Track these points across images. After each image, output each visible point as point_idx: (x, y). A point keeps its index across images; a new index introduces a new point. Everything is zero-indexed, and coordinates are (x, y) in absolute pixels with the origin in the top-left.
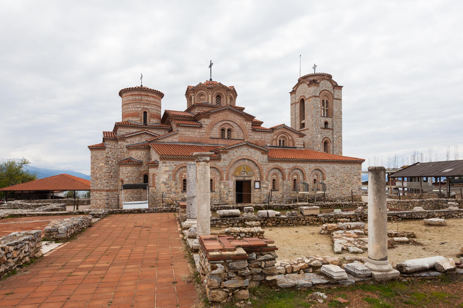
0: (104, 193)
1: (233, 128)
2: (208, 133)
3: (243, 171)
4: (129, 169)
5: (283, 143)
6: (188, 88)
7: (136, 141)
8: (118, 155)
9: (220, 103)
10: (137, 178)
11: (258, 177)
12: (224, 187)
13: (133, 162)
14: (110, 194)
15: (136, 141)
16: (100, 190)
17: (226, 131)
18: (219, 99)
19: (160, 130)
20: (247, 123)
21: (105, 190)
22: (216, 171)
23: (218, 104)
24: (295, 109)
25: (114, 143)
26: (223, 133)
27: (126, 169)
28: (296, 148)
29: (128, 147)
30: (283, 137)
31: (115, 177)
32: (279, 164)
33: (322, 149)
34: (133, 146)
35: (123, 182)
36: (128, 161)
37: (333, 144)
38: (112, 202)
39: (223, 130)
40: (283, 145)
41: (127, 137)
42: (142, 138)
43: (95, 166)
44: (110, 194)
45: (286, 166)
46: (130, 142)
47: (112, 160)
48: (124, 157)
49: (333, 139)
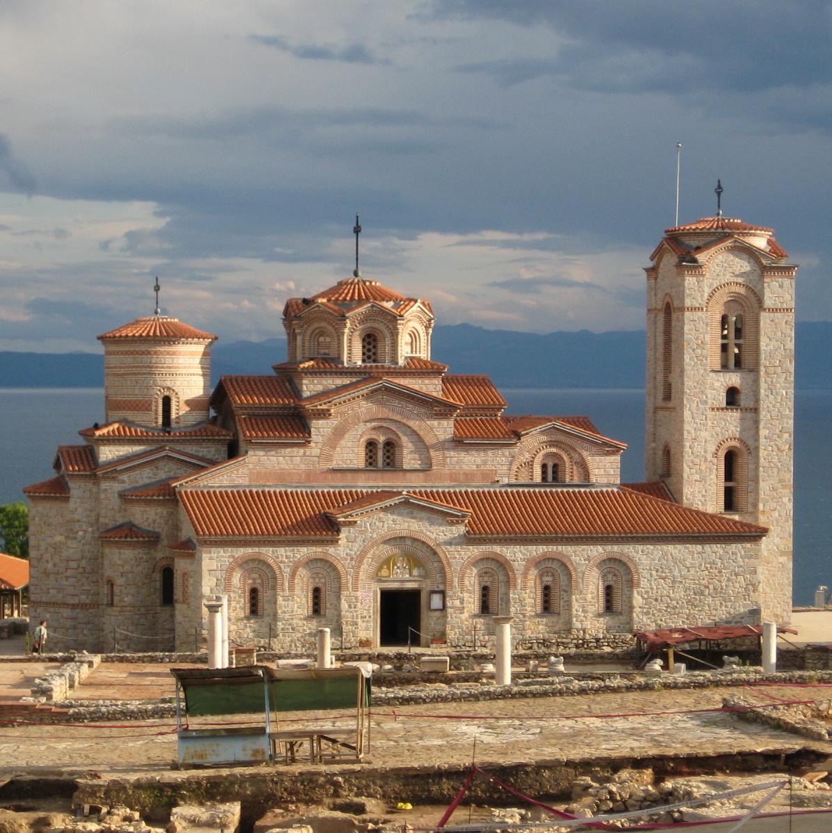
0: (66, 612)
1: (399, 438)
2: (329, 458)
3: (398, 568)
4: (128, 553)
5: (555, 472)
6: (287, 307)
7: (145, 477)
8: (98, 515)
9: (374, 354)
10: (146, 576)
11: (440, 580)
12: (347, 606)
13: (137, 537)
14: (80, 616)
15: (142, 478)
16: (55, 604)
17: (381, 446)
18: (373, 343)
19: (204, 445)
20: (439, 424)
21: (68, 604)
22: (329, 567)
23: (369, 357)
24: (655, 332)
25: (90, 485)
26: (371, 451)
27: (120, 553)
28: (592, 485)
29: (123, 496)
30: (555, 455)
31: (93, 571)
32: (497, 549)
33: (713, 476)
34: (137, 496)
35: (112, 585)
36: (124, 535)
37: (757, 457)
38: (85, 635)
39: (371, 445)
40: (555, 479)
41: (121, 470)
42: (157, 468)
43: (43, 540)
44: (80, 613)
45: (517, 555)
46: (128, 481)
47: (84, 528)
48: (115, 521)
49: (756, 437)
